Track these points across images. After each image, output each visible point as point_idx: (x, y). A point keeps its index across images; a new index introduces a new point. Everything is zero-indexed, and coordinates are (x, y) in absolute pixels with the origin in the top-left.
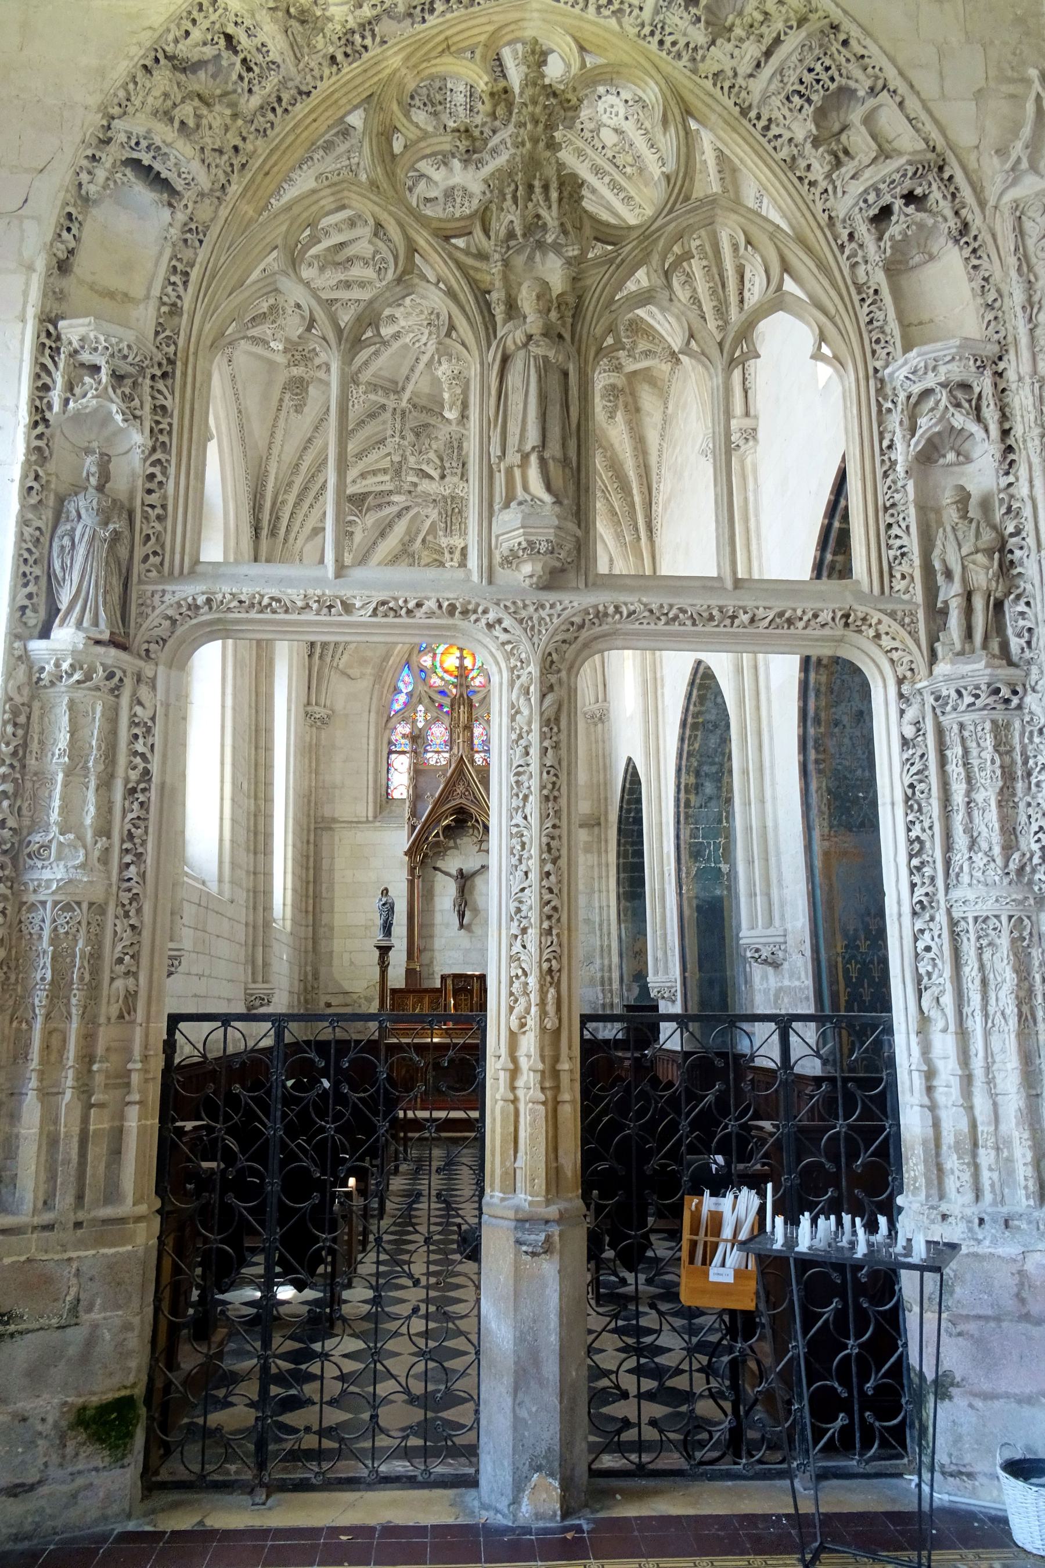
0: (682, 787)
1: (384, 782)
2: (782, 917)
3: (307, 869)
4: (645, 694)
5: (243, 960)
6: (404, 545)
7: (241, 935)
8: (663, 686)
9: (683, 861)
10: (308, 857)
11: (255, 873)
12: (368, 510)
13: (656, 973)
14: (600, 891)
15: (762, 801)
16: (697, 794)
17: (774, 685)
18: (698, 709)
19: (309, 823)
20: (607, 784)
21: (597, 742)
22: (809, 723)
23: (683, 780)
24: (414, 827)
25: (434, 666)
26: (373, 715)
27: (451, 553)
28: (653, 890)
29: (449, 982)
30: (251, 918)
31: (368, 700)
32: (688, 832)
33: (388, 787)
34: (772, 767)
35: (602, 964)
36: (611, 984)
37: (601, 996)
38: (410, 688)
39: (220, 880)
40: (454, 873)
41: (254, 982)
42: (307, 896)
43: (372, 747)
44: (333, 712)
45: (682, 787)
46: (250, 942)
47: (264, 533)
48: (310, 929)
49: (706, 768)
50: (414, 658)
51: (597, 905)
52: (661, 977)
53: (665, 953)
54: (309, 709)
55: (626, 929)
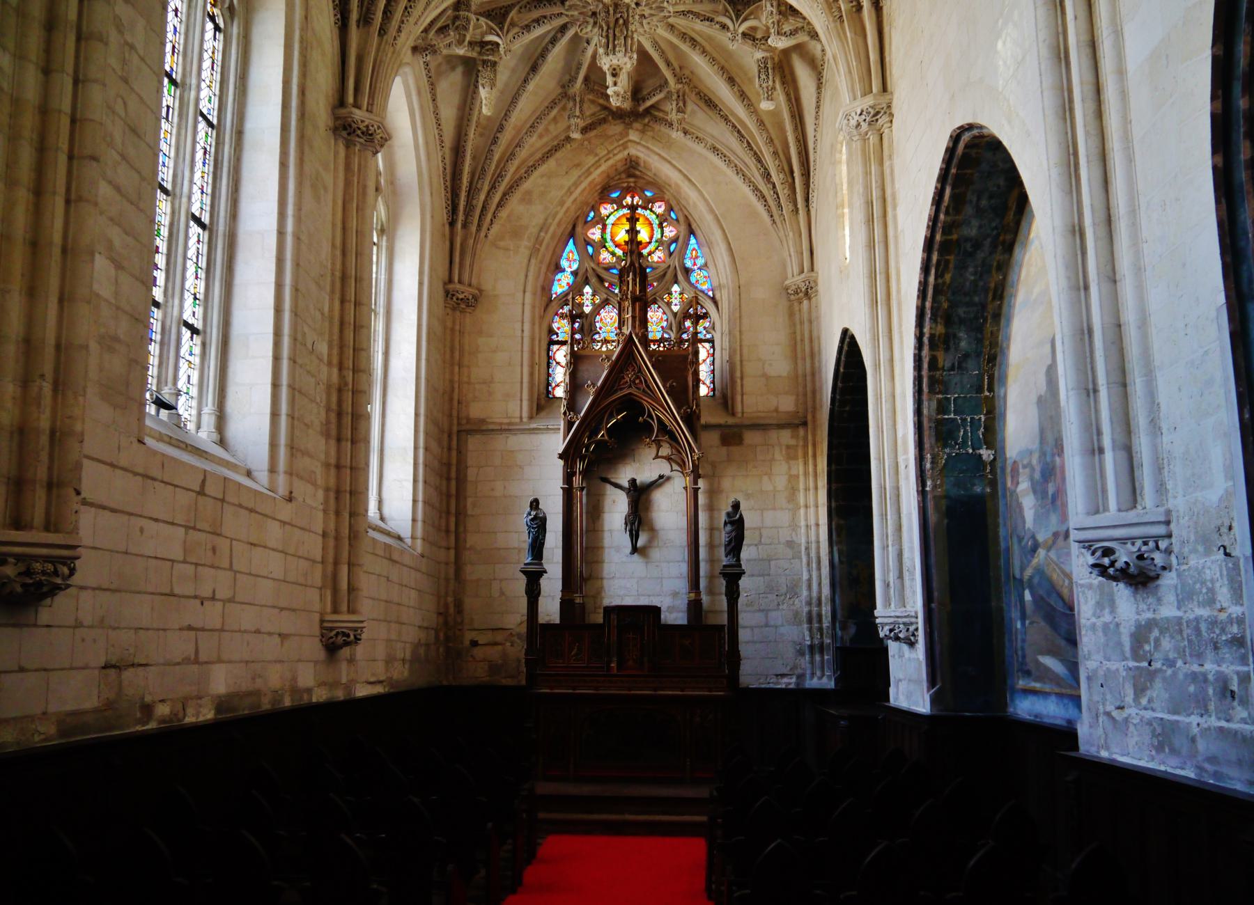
0: (926, 340)
1: (544, 376)
2: (1161, 489)
3: (449, 479)
4: (870, 220)
5: (319, 582)
6: (563, 87)
7: (314, 546)
8: (895, 208)
9: (927, 446)
10: (449, 465)
11: (338, 467)
12: (513, 24)
13: (887, 603)
14: (806, 507)
15: (1112, 278)
16: (947, 349)
17: (1131, 66)
18: (949, 219)
19: (451, 425)
20: (815, 373)
21: (802, 323)
22: (1237, 88)
23: (926, 330)
24: (570, 424)
25: (603, 240)
26: (528, 296)
27: (614, 75)
28: (883, 489)
29: (614, 617)
30: (332, 526)
31: (522, 277)
32: (934, 404)
33: (549, 384)
34: (1133, 212)
35: (810, 596)
36: (820, 621)
37: (808, 638)
38: (575, 266)
39: (273, 470)
40: (626, 485)
41: (335, 611)
42: (448, 513)
43: (527, 334)
44: (481, 291)
45: (926, 340)
46: (330, 559)
47: (354, 16)
48: (452, 552)
49: (961, 311)
50: (579, 229)
51: (803, 523)
52: (894, 610)
53: (901, 576)
54: (450, 287)
55: (840, 553)
